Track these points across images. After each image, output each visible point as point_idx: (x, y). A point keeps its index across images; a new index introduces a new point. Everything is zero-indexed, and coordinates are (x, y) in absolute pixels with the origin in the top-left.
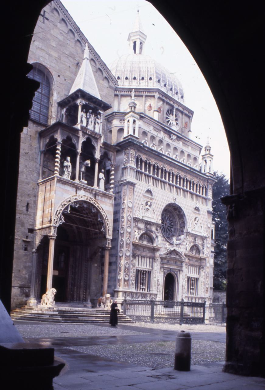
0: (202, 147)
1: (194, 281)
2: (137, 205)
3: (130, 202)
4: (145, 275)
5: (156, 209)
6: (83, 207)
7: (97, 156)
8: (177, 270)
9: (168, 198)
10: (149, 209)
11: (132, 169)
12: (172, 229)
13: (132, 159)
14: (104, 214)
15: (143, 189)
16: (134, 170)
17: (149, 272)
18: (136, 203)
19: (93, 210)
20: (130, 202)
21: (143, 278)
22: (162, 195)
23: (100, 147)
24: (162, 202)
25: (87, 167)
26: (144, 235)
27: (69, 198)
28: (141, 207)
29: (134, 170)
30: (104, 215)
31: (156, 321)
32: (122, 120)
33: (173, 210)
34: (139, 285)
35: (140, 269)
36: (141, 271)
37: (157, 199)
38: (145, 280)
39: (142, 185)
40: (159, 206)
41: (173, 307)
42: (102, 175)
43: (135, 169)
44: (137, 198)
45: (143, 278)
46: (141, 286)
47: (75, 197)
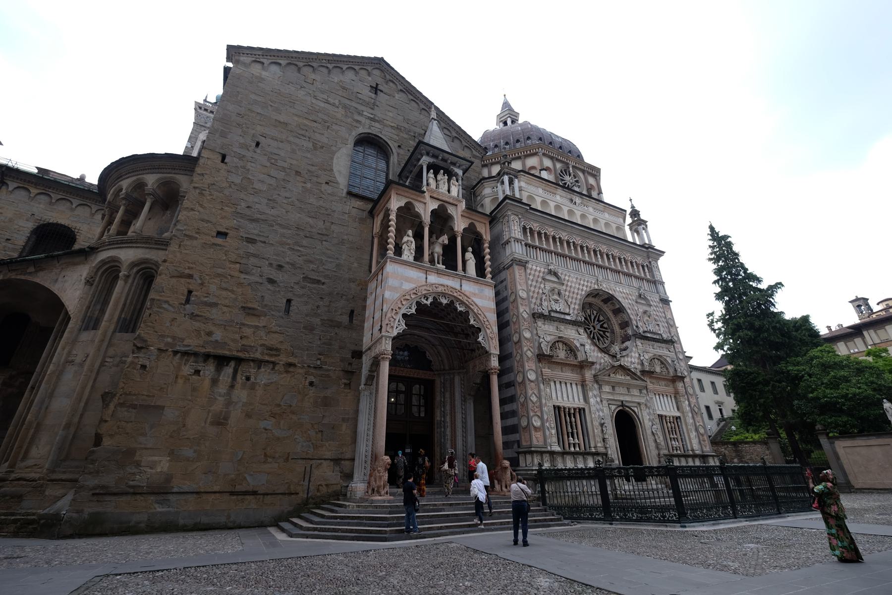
0: (625, 211)
1: (673, 422)
2: (535, 295)
3: (523, 290)
4: (574, 417)
5: (570, 300)
6: (441, 304)
7: (458, 228)
8: (636, 405)
9: (588, 282)
10: (558, 300)
11: (517, 242)
12: (608, 334)
13: (516, 228)
14: (480, 312)
15: (542, 270)
16: (521, 243)
17: (580, 410)
18: (534, 292)
19: (459, 308)
20: (523, 290)
21: (571, 422)
22: (577, 279)
23: (462, 216)
24: (578, 289)
25: (445, 247)
26: (557, 344)
27: (414, 289)
28: (544, 297)
29: (521, 243)
30: (480, 315)
31: (618, 517)
32: (495, 188)
33: (602, 303)
34: (566, 437)
35: (561, 405)
36: (564, 408)
37: (569, 284)
38: (576, 425)
39: (537, 265)
40: (575, 296)
41: (645, 480)
42: (469, 255)
43: (523, 241)
44: (534, 283)
45: (571, 422)
46: (571, 439)
47: (425, 287)
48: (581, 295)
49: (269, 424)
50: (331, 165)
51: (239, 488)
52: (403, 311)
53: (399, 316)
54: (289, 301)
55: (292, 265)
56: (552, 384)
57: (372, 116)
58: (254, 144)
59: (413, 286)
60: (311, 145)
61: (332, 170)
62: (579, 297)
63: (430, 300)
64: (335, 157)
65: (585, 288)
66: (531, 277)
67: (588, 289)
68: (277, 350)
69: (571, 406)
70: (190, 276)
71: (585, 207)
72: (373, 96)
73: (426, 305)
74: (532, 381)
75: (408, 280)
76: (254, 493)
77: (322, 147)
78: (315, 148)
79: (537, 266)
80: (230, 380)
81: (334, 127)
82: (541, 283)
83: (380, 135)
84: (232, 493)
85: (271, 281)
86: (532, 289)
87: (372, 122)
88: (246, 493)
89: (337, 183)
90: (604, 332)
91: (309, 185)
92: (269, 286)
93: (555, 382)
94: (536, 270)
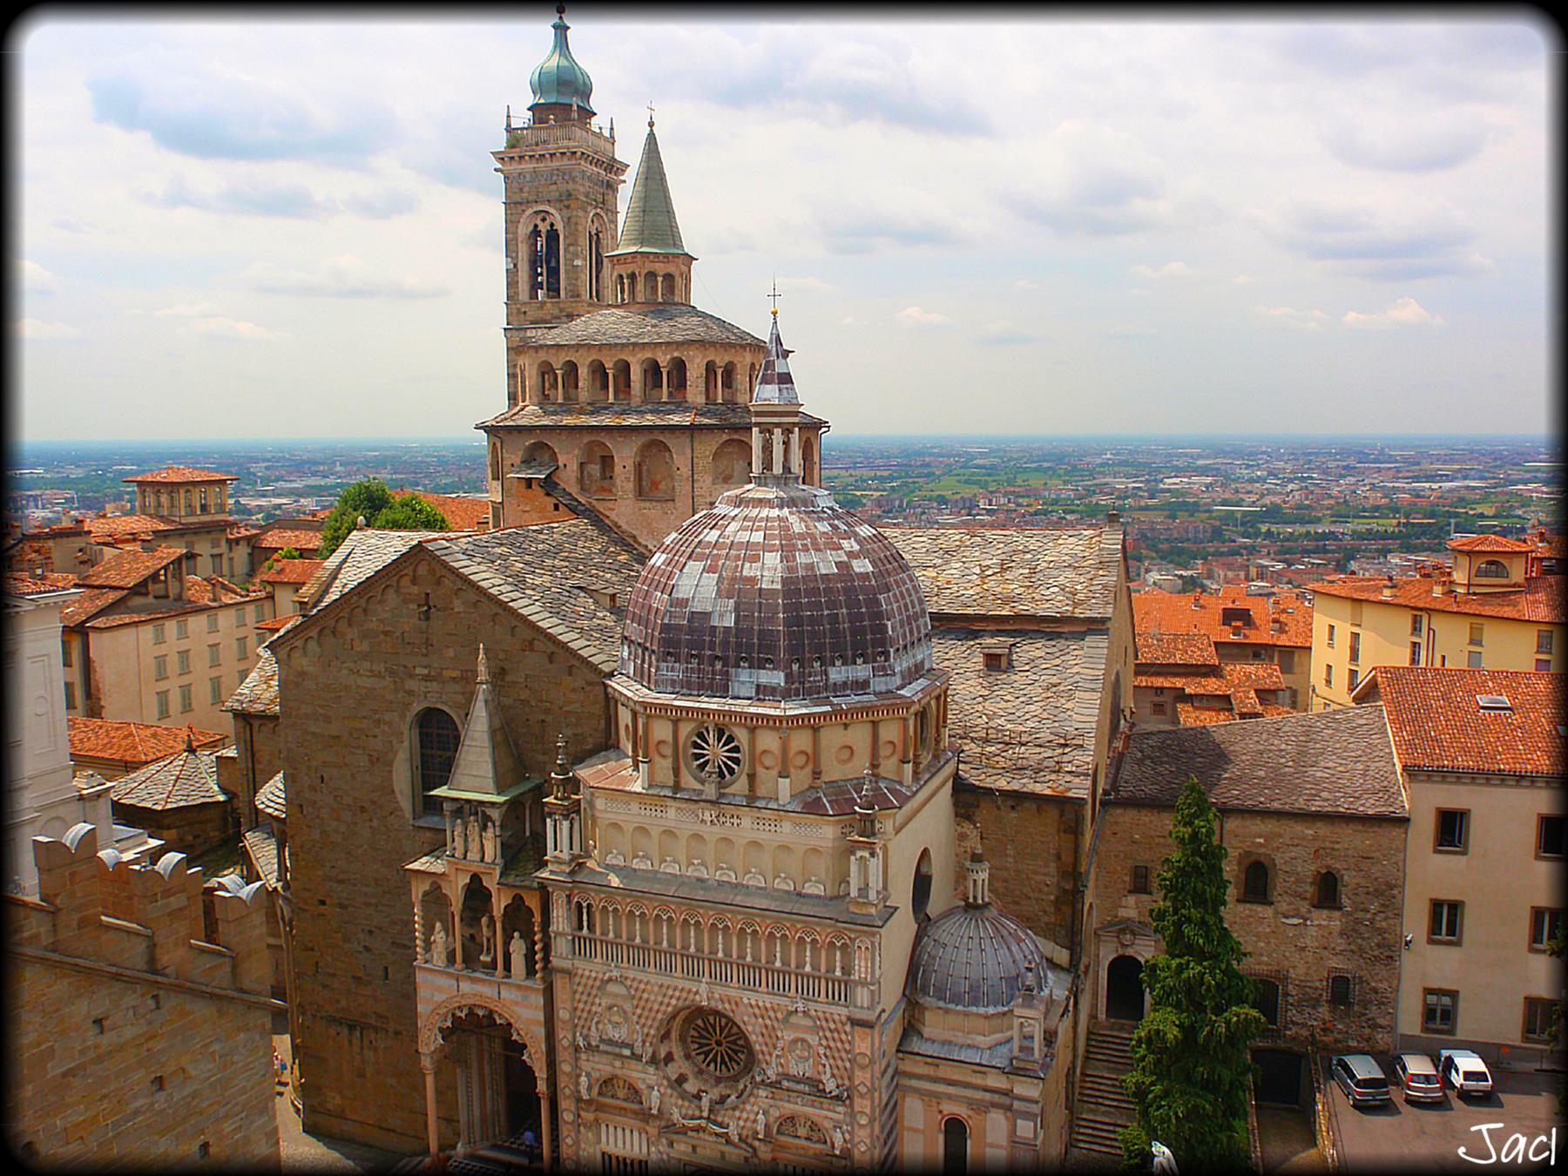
15: (600, 975)
36: (617, 1157)
44: (584, 998)
47: (456, 999)
48: (665, 1013)
49: (391, 1081)
50: (391, 785)
51: (383, 1125)
52: (439, 1025)
53: (437, 1031)
54: (386, 968)
55: (380, 929)
56: (603, 1126)
57: (426, 672)
58: (319, 780)
59: (444, 997)
60: (367, 758)
61: (393, 791)
62: (660, 1016)
63: (465, 1011)
64: (394, 769)
65: (674, 1002)
66: (580, 989)
67: (681, 1004)
68: (386, 1018)
69: (626, 1155)
70: (312, 949)
71: (735, 821)
72: (424, 624)
73: (461, 1017)
74: (567, 1123)
75: (440, 989)
76: (394, 1131)
77: (378, 759)
78: (372, 763)
79: (591, 971)
80: (359, 1043)
81: (388, 717)
82: (596, 996)
83: (439, 706)
84: (381, 1128)
85: (367, 948)
86: (581, 1006)
87: (429, 684)
88: (388, 1130)
89: (401, 810)
90: (736, 1052)
91: (375, 823)
92: (367, 955)
93: (607, 1126)
94: (589, 977)
